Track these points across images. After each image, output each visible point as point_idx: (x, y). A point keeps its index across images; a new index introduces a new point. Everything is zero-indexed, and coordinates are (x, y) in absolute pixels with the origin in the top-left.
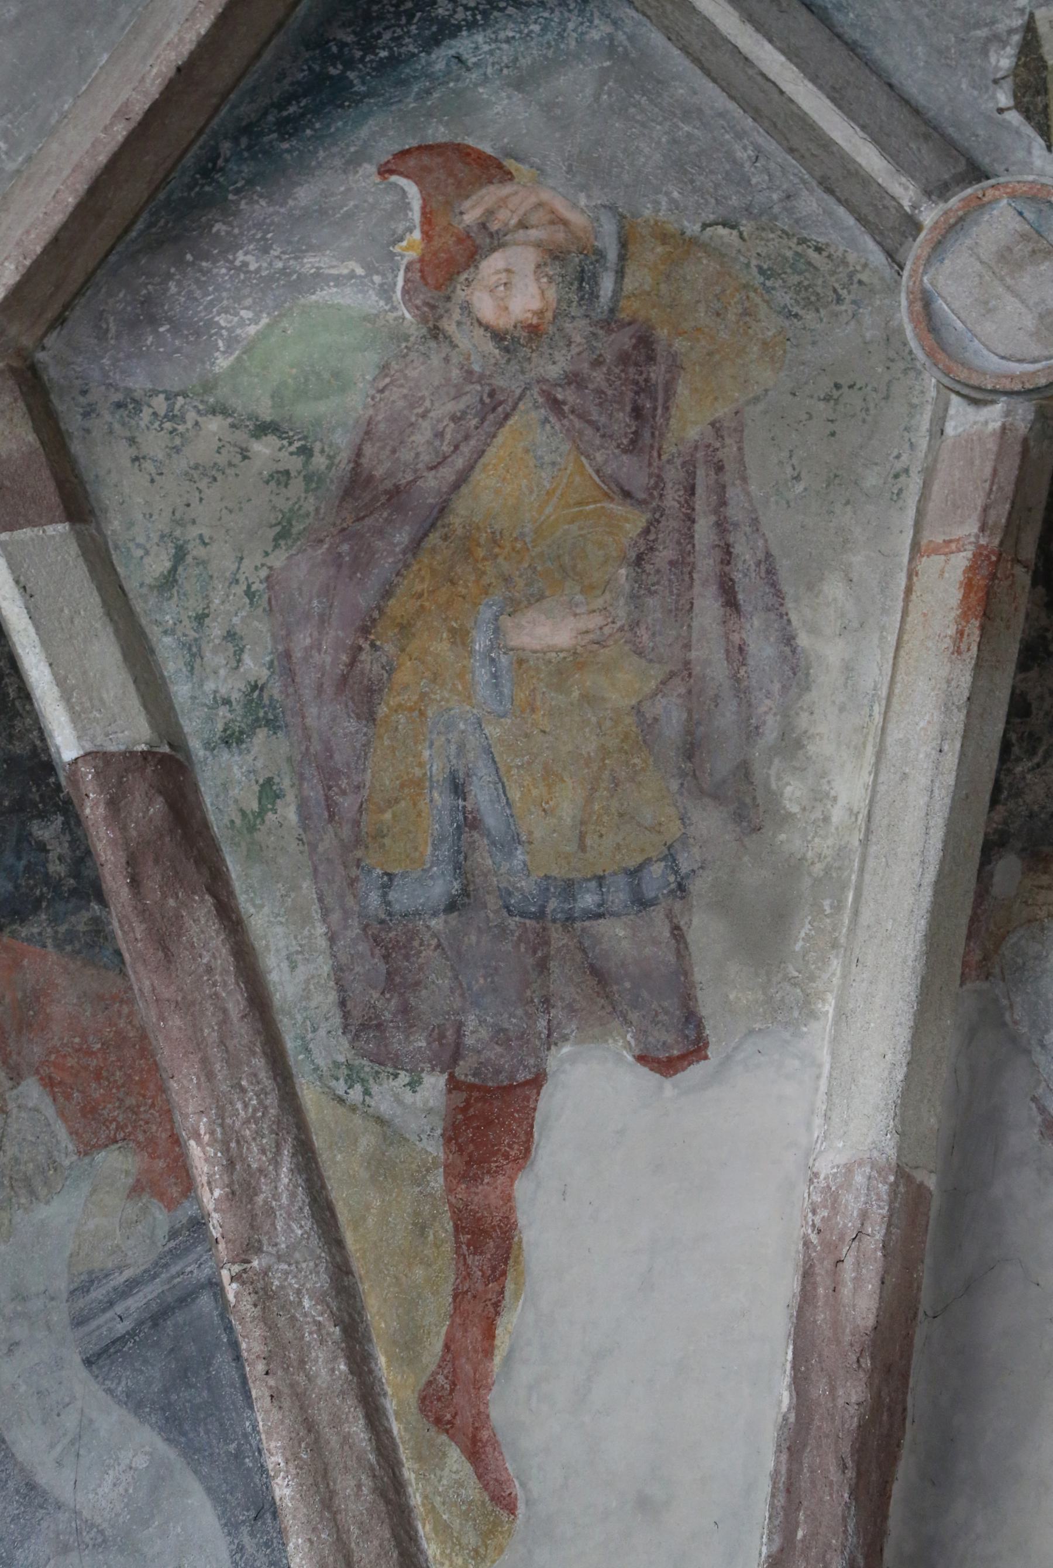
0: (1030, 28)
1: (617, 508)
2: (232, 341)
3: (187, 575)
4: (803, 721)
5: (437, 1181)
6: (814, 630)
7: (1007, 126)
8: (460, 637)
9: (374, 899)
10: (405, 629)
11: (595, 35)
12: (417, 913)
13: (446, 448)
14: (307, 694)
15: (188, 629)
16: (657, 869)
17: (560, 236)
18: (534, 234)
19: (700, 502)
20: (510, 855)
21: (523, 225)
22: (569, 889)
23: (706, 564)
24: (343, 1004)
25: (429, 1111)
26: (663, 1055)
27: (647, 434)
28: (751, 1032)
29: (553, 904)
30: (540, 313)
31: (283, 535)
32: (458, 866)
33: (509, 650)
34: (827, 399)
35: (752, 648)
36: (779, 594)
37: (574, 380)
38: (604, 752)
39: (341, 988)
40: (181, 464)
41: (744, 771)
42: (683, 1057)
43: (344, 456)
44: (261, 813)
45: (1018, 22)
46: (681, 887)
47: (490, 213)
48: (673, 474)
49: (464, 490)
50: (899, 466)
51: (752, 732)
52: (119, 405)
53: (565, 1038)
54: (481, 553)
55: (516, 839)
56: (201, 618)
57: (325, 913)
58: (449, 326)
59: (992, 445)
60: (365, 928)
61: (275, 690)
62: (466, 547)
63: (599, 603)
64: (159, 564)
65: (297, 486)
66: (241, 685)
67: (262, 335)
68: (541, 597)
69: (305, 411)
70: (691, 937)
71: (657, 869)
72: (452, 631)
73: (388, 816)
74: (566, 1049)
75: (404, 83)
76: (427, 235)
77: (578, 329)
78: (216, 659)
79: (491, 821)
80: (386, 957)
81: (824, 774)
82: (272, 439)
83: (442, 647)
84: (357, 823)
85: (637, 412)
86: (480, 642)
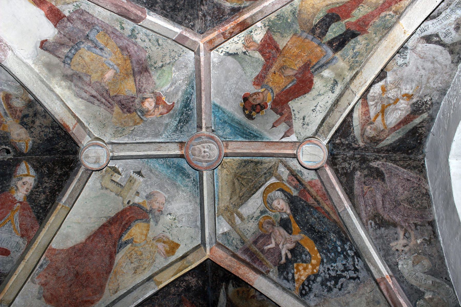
0: (120, 175)
1: (115, 94)
2: (174, 72)
3: (156, 43)
4: (71, 92)
5: (53, 3)
6: (81, 101)
7: (113, 164)
8: (118, 65)
9: (98, 28)
10: (125, 60)
11: (164, 135)
12: (91, 31)
13: (140, 82)
14: (129, 43)
15: (150, 37)
16: (69, 62)
17: (149, 114)
18: (152, 111)
19: (107, 103)
20: (87, 47)
21: (154, 111)
22: (76, 50)
23: (99, 97)
24: (88, 13)
25: (64, 10)
26: (44, 43)
27: (120, 104)
28: (38, 55)
29: (76, 47)
30: (143, 105)
31: (149, 57)
32: (92, 41)
33: (111, 69)
34: (105, 124)
35: (85, 94)
36: (88, 102)
37: (133, 102)
38: (89, 68)
39: (90, 15)
40: (168, 54)
41: (72, 81)
42: (42, 45)
43: (151, 72)
44: (121, 25)
45: (122, 174)
46: (64, 62)
47: (159, 109)
48: (113, 102)
49: (134, 80)
50: (90, 125)
51: (76, 85)
52: (181, 54)
53: (58, 34)
54: (125, 76)
55: (88, 50)
56: (150, 40)
57: (102, 21)
58: (152, 95)
59: (81, 141)
60: (95, 24)
61: (133, 40)
62: (127, 75)
63: (107, 83)
64: (160, 42)
65: (153, 64)
66: (138, 37)
67: (171, 76)
68: (114, 77)
69: (159, 72)
70: (57, 58)
71: (69, 62)
72: (120, 65)
73: (106, 39)
74: (56, 33)
75: (179, 114)
76: (163, 101)
77: (138, 107)
78: (144, 37)
79: (94, 49)
80: (89, 23)
81: (63, 88)
82: (160, 66)
83: (119, 62)
84: (109, 34)
85: (123, 105)
86: (115, 67)
